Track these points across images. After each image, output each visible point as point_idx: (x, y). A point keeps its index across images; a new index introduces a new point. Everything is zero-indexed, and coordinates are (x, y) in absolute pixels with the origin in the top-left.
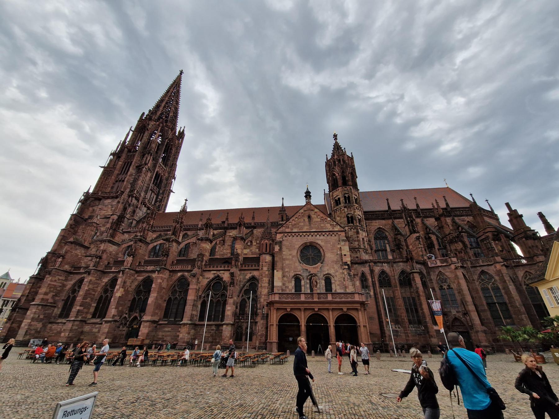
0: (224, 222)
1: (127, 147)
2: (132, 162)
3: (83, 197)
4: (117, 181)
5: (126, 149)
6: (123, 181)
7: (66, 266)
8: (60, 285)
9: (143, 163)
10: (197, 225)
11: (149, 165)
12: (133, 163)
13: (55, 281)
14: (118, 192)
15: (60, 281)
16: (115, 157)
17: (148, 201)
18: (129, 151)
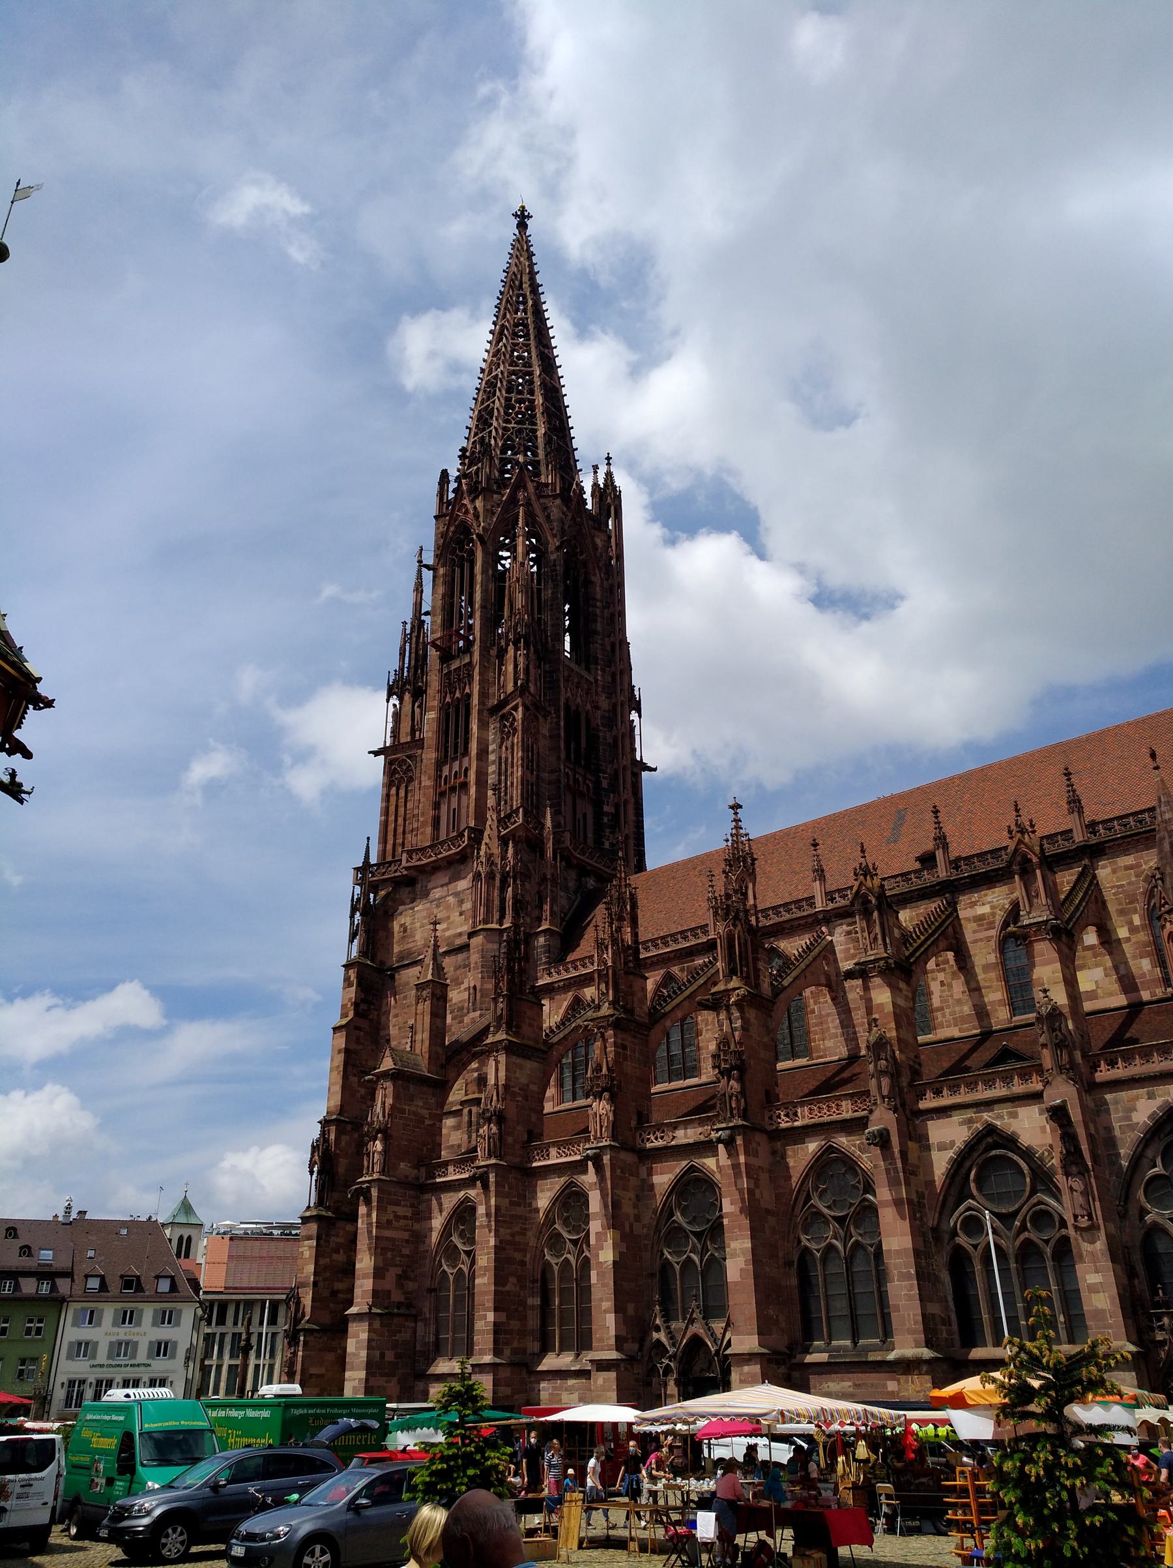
0: (927, 860)
1: (433, 644)
2: (469, 696)
3: (358, 890)
4: (442, 794)
5: (432, 653)
6: (464, 786)
7: (402, 1165)
8: (406, 1236)
9: (510, 688)
10: (810, 900)
11: (532, 689)
12: (475, 700)
13: (389, 1222)
14: (461, 835)
15: (403, 1222)
16: (407, 696)
17: (574, 836)
18: (446, 657)
